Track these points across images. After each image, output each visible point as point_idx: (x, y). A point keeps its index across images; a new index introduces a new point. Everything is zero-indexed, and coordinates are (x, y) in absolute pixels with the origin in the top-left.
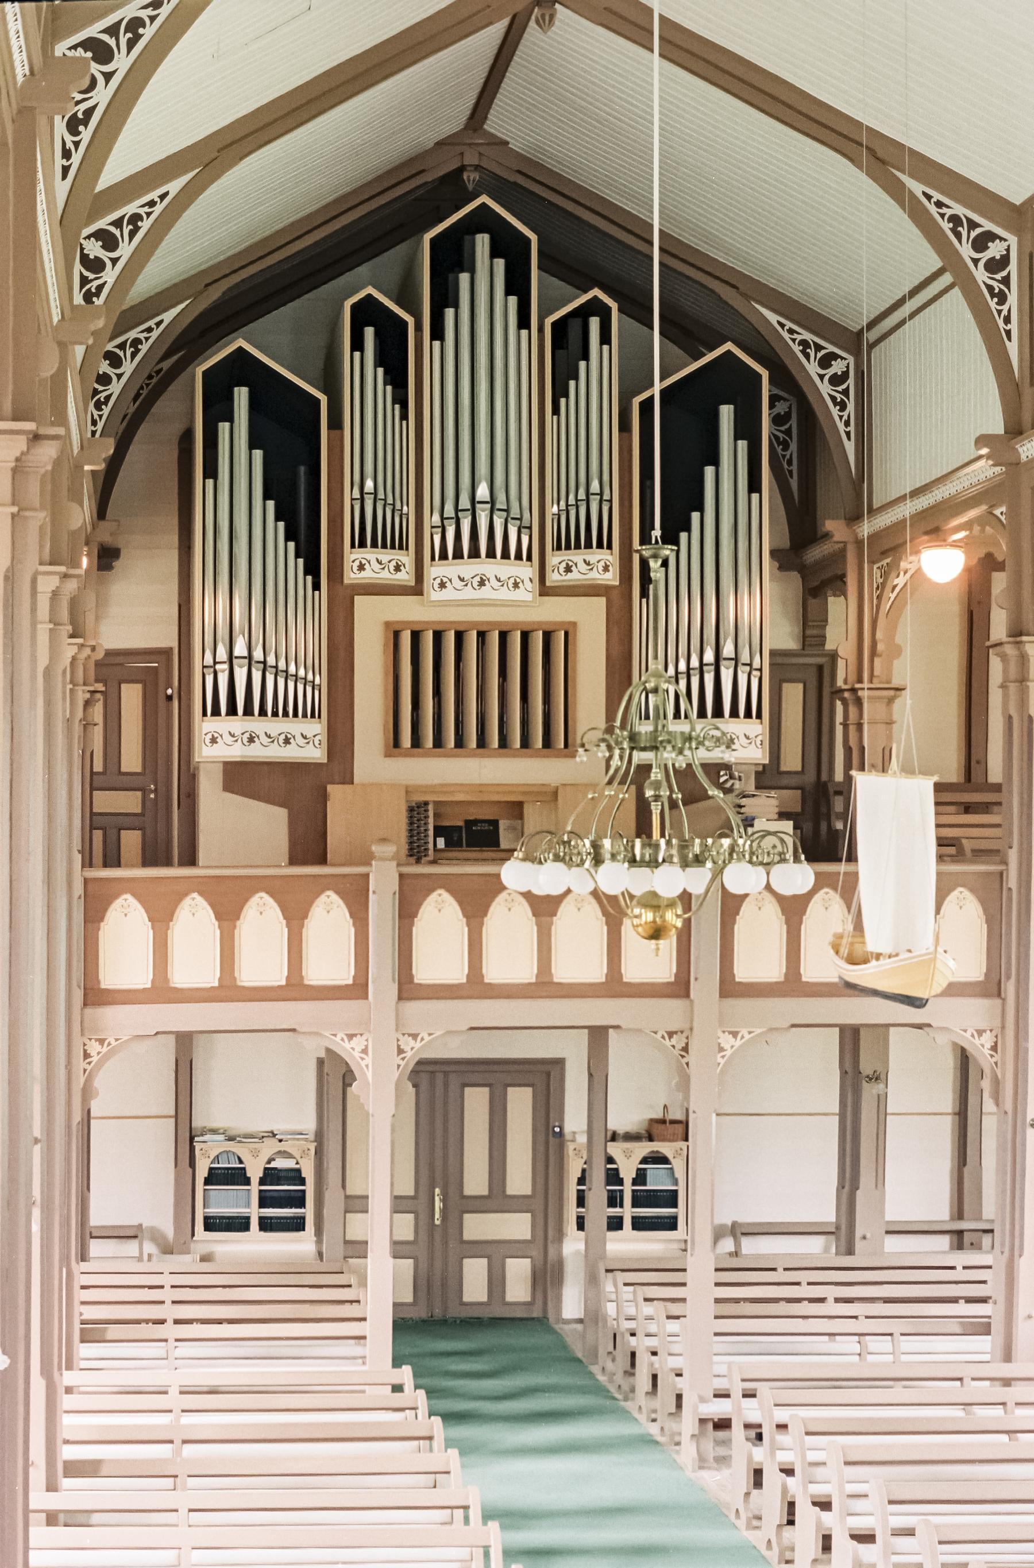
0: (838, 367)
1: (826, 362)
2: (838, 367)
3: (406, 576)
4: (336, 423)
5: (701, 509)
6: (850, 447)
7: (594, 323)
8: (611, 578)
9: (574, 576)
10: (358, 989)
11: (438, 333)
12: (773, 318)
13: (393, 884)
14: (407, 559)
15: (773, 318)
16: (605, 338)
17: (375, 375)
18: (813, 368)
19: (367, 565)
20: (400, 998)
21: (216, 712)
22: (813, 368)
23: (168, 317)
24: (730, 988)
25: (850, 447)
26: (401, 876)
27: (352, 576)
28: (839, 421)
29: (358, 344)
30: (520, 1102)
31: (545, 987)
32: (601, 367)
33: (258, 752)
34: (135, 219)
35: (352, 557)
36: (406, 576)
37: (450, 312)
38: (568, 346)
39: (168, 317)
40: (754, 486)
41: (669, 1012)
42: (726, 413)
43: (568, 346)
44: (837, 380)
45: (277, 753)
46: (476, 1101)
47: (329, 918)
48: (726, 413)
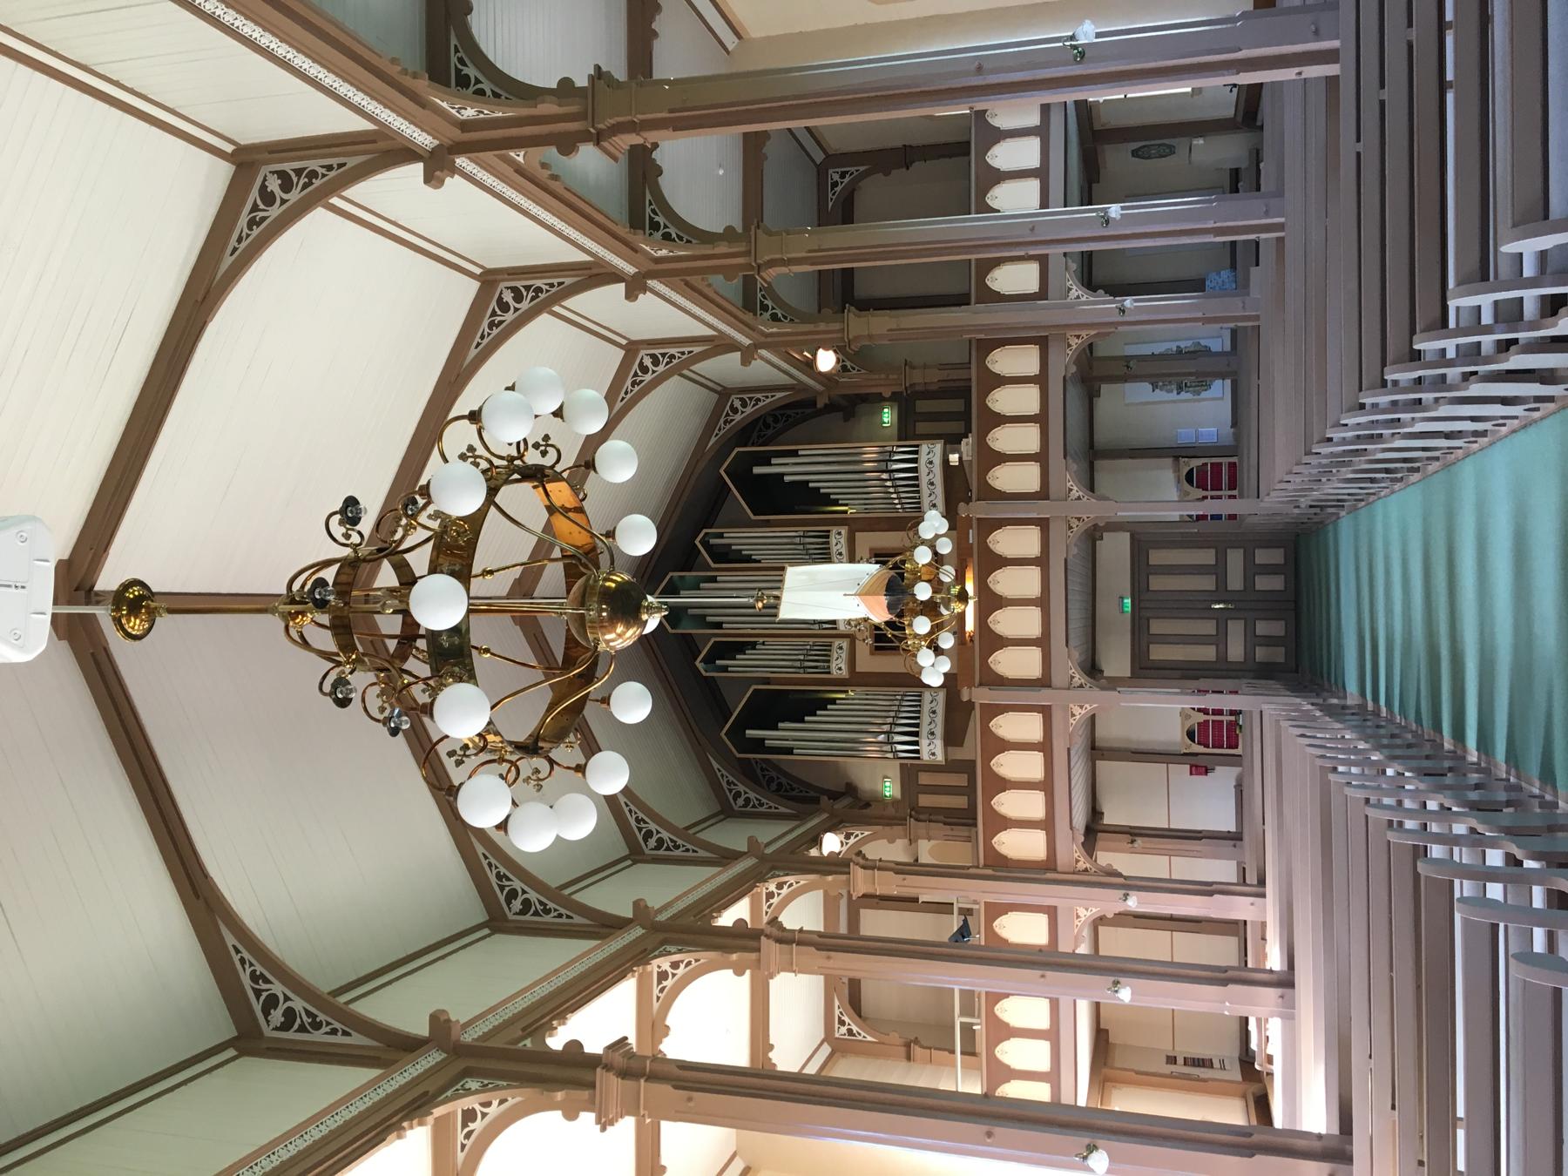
0: (737, 404)
1: (735, 411)
2: (737, 404)
3: (845, 644)
4: (767, 681)
5: (808, 482)
6: (779, 395)
7: (713, 541)
8: (844, 530)
9: (844, 551)
10: (1046, 712)
11: (719, 625)
12: (713, 440)
13: (985, 690)
14: (837, 642)
15: (713, 440)
16: (721, 536)
17: (742, 660)
18: (738, 417)
19: (839, 666)
20: (1050, 686)
21: (917, 752)
22: (738, 417)
23: (716, 765)
24: (1043, 494)
25: (779, 395)
26: (981, 684)
27: (845, 673)
28: (766, 401)
29: (725, 669)
30: (1157, 557)
31: (1043, 602)
32: (736, 538)
33: (939, 731)
34: (638, 820)
35: (835, 673)
36: (845, 644)
37: (709, 619)
38: (726, 556)
39: (716, 765)
40: (795, 454)
41: (1056, 530)
42: (757, 470)
43: (726, 556)
44: (744, 405)
45: (940, 718)
46: (1157, 583)
48: (757, 470)
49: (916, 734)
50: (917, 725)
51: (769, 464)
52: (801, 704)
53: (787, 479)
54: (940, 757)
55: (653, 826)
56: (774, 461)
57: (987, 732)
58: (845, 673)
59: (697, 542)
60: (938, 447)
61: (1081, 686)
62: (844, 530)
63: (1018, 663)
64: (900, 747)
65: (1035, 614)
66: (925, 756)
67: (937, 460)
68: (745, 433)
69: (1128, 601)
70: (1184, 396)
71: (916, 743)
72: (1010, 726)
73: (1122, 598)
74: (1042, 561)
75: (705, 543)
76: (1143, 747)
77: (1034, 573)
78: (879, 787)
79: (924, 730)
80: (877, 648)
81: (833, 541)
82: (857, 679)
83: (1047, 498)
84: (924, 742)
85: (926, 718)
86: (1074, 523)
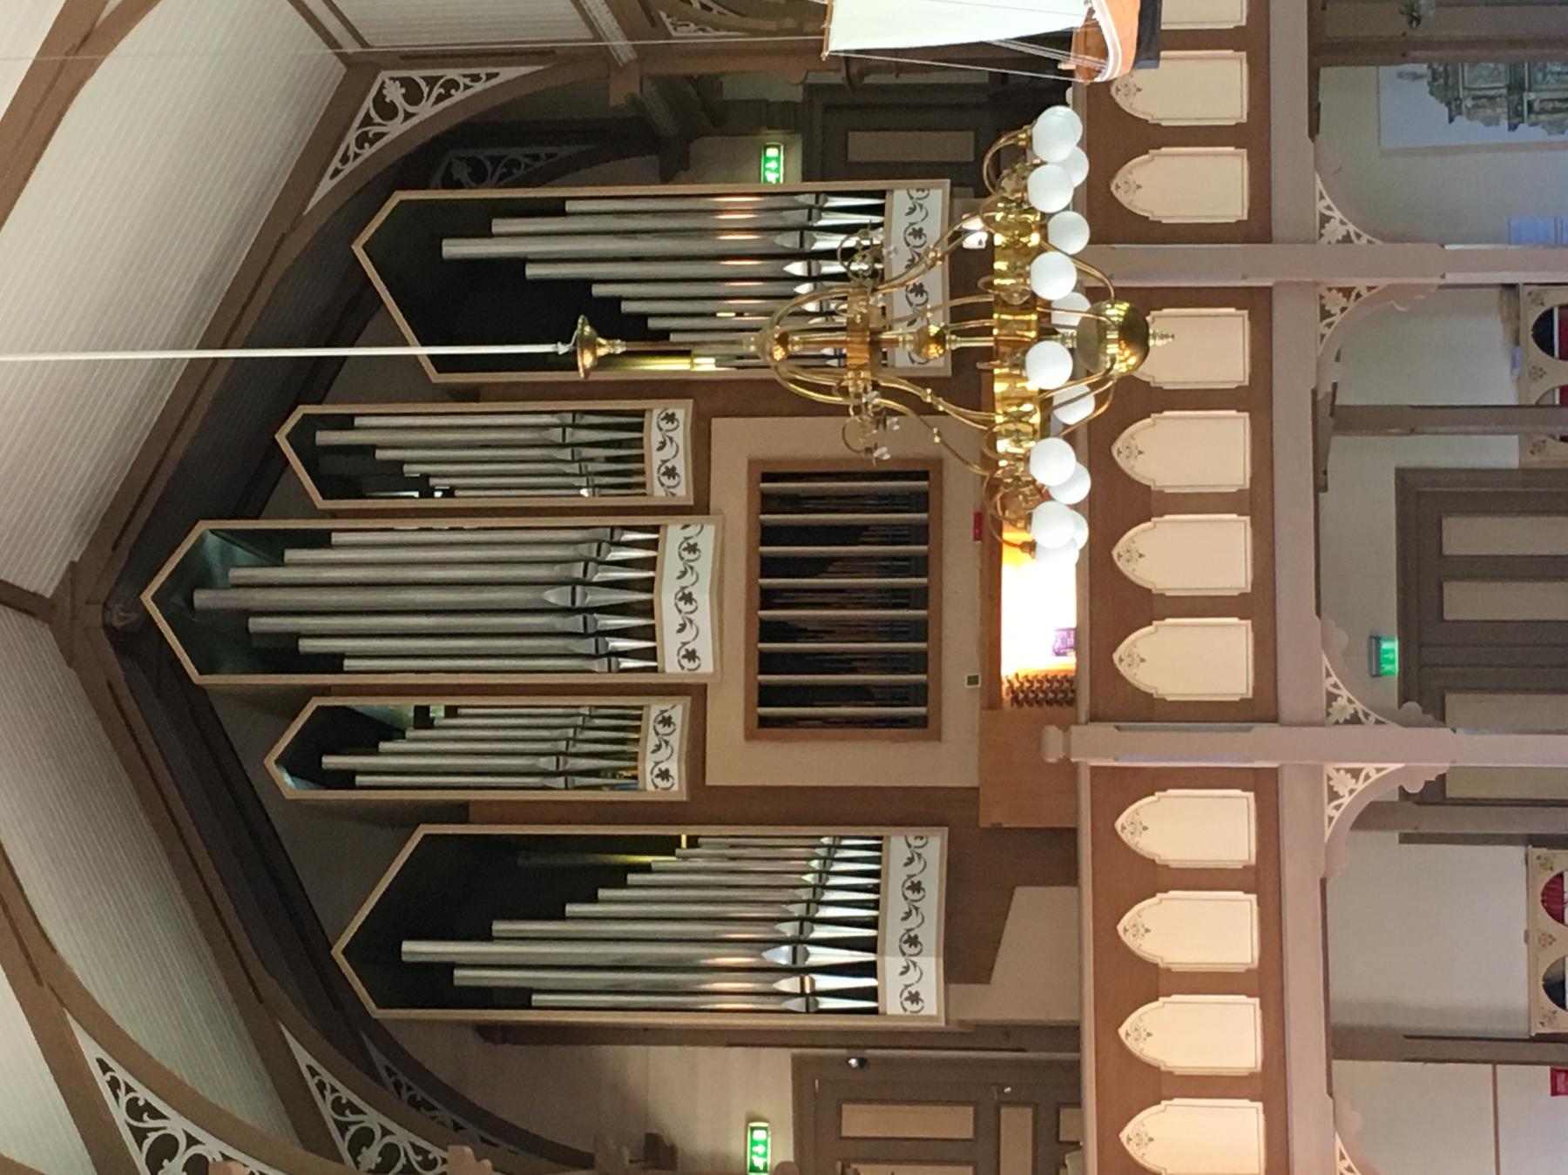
0: (395, 94)
1: (387, 110)
2: (395, 94)
3: (678, 710)
4: (460, 812)
5: (588, 283)
6: (508, 73)
7: (325, 437)
8: (682, 411)
9: (681, 465)
10: (1264, 787)
11: (333, 663)
12: (326, 185)
13: (1104, 731)
14: (655, 708)
15: (326, 185)
16: (346, 422)
17: (391, 756)
18: (395, 128)
19: (661, 769)
20: (1274, 719)
21: (871, 993)
22: (395, 128)
24: (1256, 229)
25: (508, 73)
26: (1094, 718)
27: (676, 788)
28: (474, 87)
29: (345, 779)
30: (1465, 536)
31: (1255, 502)
32: (380, 427)
33: (931, 932)
34: (134, 1109)
35: (651, 787)
36: (678, 710)
37: (306, 645)
38: (358, 477)
40: (555, 209)
42: (454, 249)
43: (358, 477)
44: (413, 94)
45: (932, 901)
46: (1466, 602)
47: (1166, 827)
48: (454, 249)
49: (869, 945)
50: (869, 945)
51: (486, 233)
52: (544, 872)
53: (532, 271)
54: (931, 1006)
55: (176, 1125)
56: (499, 226)
57: (1111, 844)
58: (676, 788)
59: (281, 438)
60: (936, 196)
61: (1354, 720)
62: (682, 411)
63: (1196, 660)
64: (825, 982)
65: (1235, 531)
66: (892, 1004)
67: (934, 228)
68: (423, 161)
69: (1391, 647)
70: (1527, 132)
71: (869, 969)
72: (1166, 827)
73: (1377, 639)
74: (1253, 398)
75: (302, 438)
76: (1428, 1025)
77: (1234, 427)
78: (735, 1147)
79: (893, 930)
80: (764, 722)
81: (653, 436)
82: (710, 804)
83: (1266, 238)
84: (891, 964)
85: (895, 904)
86: (1335, 302)
